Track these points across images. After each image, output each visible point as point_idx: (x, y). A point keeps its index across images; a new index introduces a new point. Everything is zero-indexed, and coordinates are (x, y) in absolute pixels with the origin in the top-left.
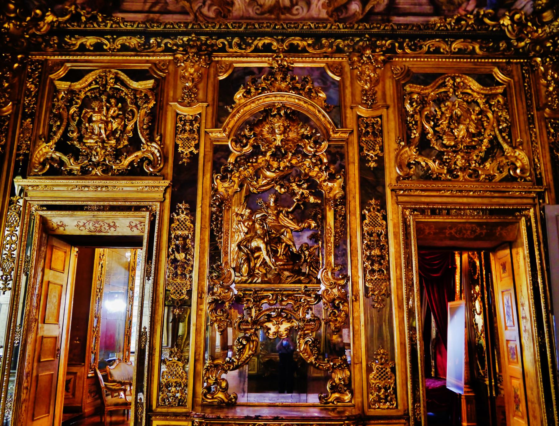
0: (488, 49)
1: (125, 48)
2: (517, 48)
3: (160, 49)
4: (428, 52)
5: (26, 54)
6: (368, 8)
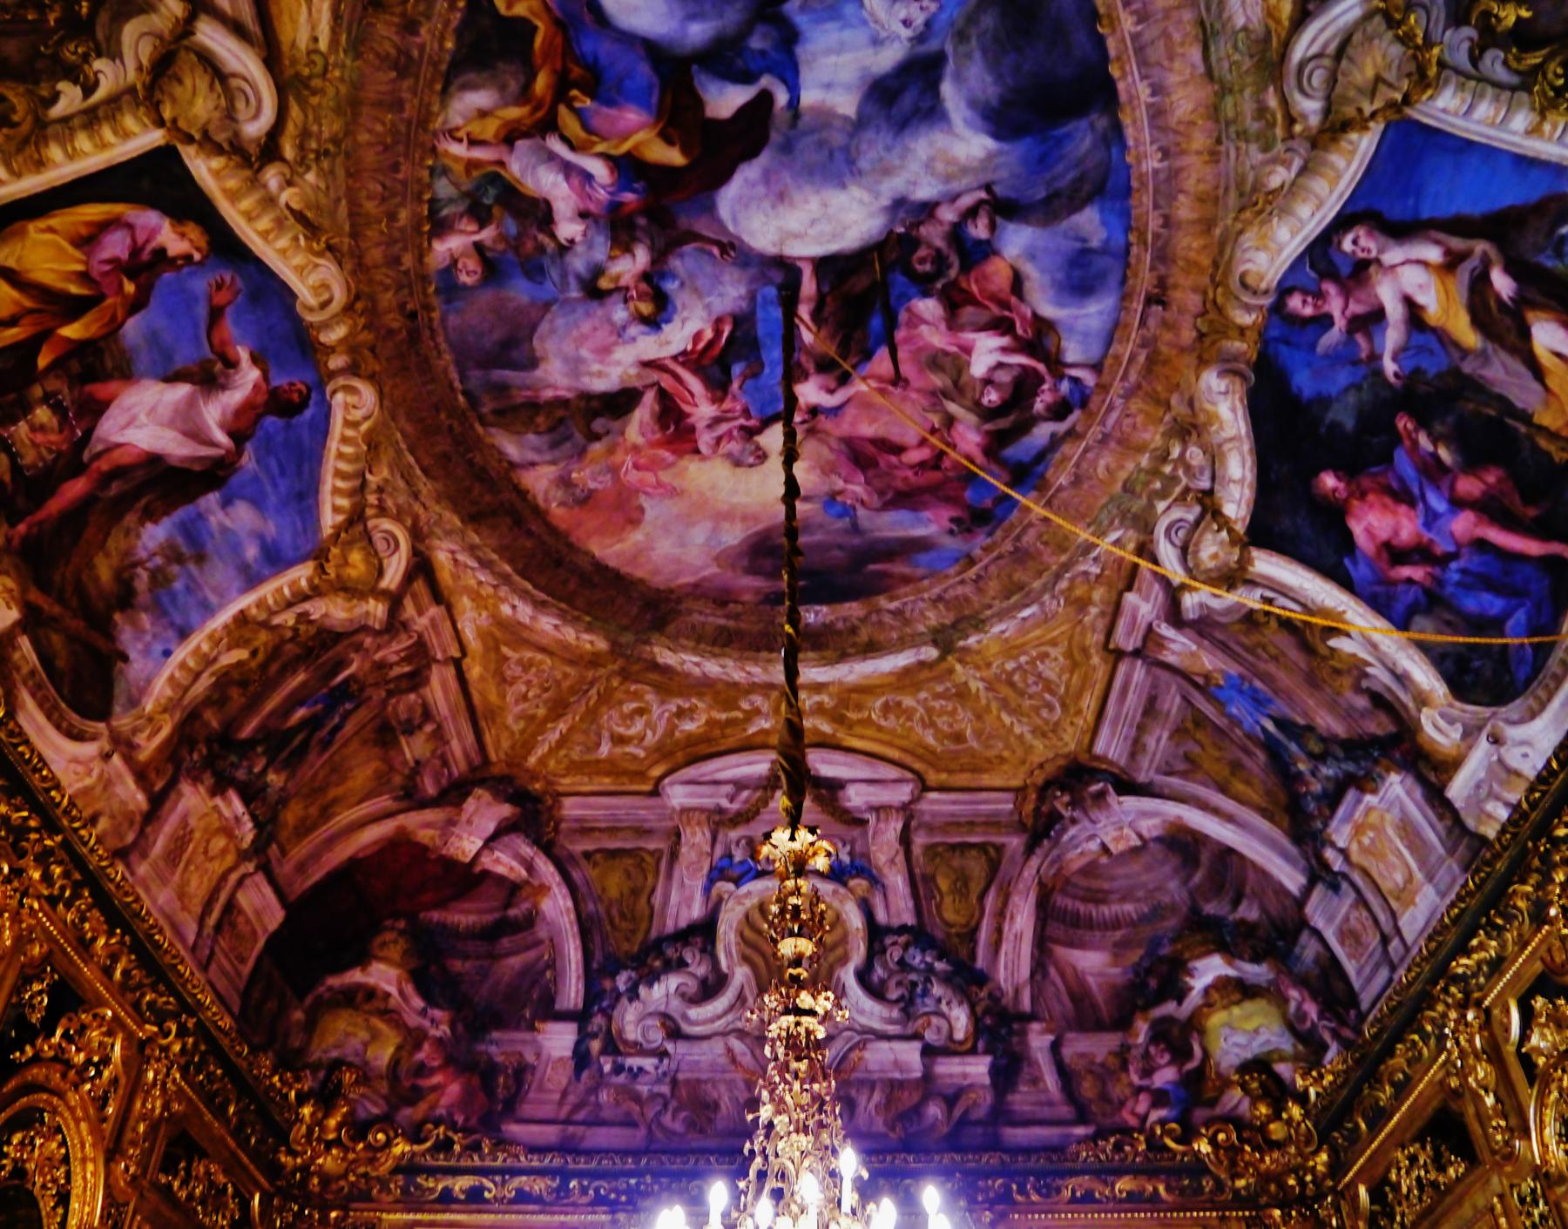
0: (1182, 1191)
1: (522, 1197)
2: (1236, 1192)
3: (584, 1200)
4: (1073, 1200)
5: (345, 1209)
6: (957, 1113)
